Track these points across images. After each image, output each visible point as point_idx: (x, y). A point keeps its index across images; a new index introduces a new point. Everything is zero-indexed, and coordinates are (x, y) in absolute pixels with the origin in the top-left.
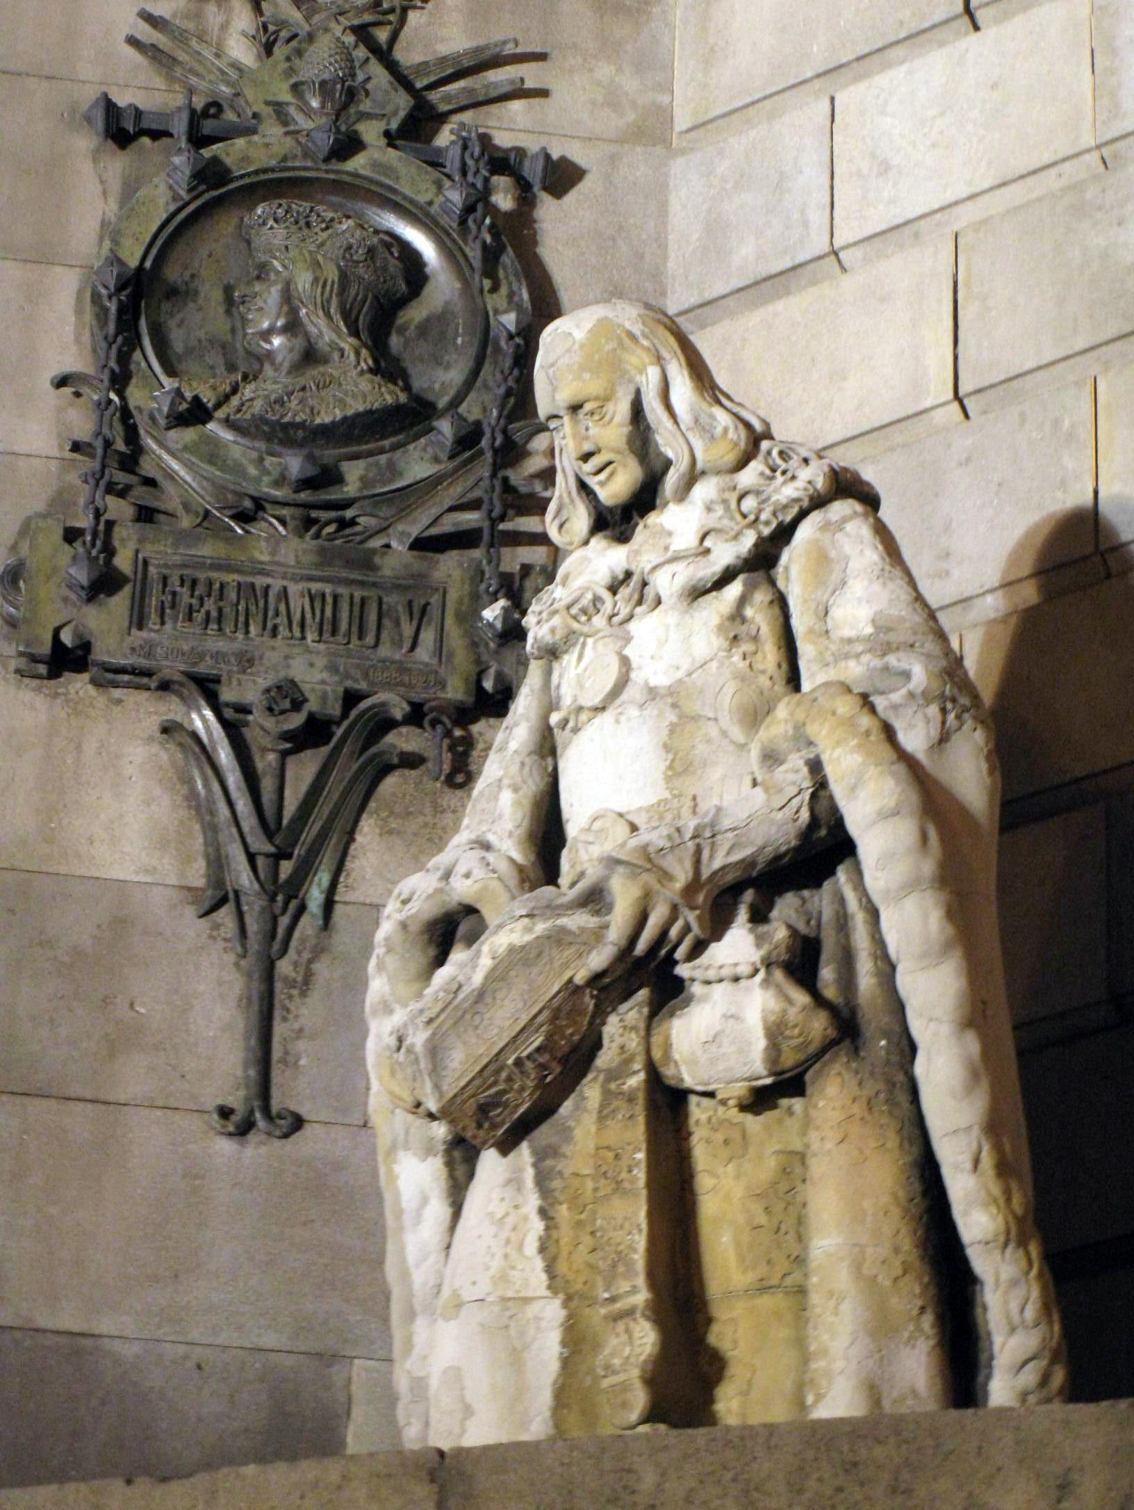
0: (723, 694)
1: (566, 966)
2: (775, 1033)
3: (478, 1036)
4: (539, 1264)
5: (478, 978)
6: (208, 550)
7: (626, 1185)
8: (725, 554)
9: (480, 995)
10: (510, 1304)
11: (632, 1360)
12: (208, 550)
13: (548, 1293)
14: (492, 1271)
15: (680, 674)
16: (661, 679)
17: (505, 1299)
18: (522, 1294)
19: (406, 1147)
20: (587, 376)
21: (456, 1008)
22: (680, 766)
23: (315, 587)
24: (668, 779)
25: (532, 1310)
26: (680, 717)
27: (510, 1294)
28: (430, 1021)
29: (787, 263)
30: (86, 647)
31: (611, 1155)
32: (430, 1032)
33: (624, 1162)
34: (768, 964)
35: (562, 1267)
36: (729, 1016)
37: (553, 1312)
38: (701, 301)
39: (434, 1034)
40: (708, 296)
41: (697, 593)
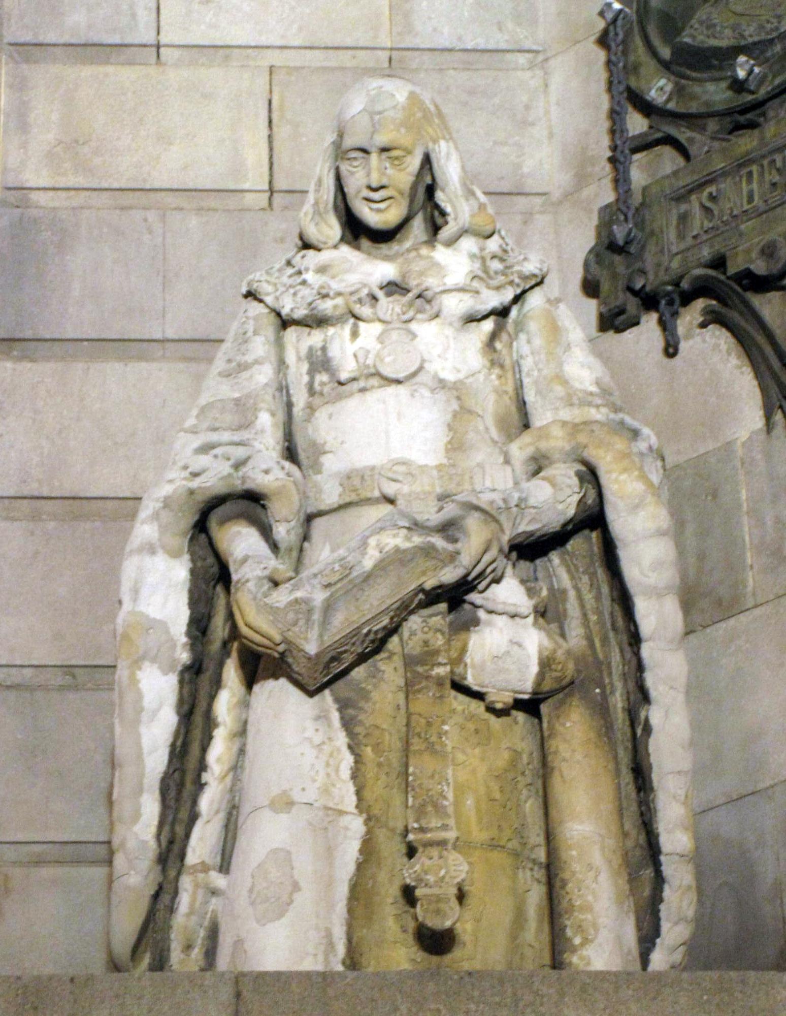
1: (424, 573)
2: (546, 664)
3: (357, 607)
4: (351, 788)
5: (368, 563)
7: (437, 747)
9: (368, 577)
10: (330, 812)
11: (447, 879)
13: (355, 811)
14: (317, 784)
15: (461, 376)
17: (327, 808)
18: (340, 807)
19: (154, 660)
20: (403, 130)
21: (351, 581)
22: (456, 445)
24: (447, 451)
25: (345, 820)
26: (461, 407)
27: (331, 805)
28: (328, 586)
29: (117, 39)
31: (423, 721)
32: (328, 594)
33: (433, 731)
35: (367, 794)
36: (508, 644)
37: (356, 826)
38: (34, 41)
39: (331, 595)
40: (41, 39)
41: (473, 319)
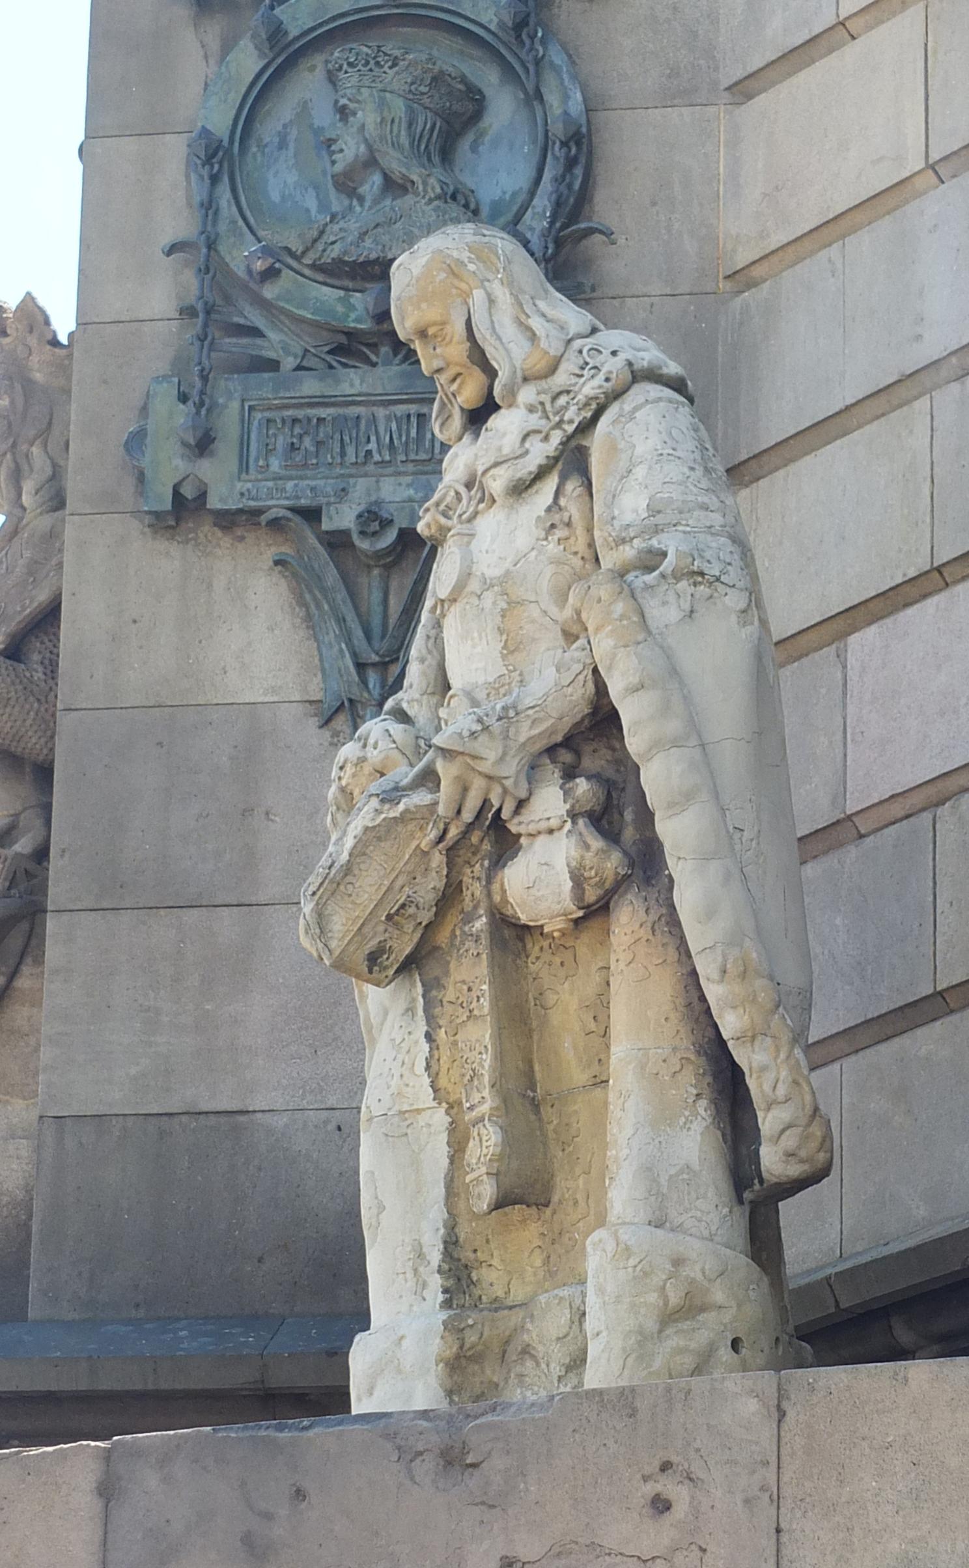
0: (541, 579)
1: (412, 836)
3: (353, 903)
5: (345, 856)
6: (310, 386)
8: (539, 452)
9: (348, 869)
10: (407, 1115)
12: (310, 386)
13: (434, 1104)
15: (508, 564)
16: (493, 572)
18: (415, 1107)
20: (424, 306)
21: (332, 881)
23: (400, 409)
24: (504, 657)
25: (422, 1120)
27: (406, 1108)
28: (314, 893)
29: (805, 36)
30: (202, 496)
31: (465, 987)
33: (474, 994)
34: (573, 815)
37: (440, 1118)
38: (746, 74)
39: (317, 904)
40: (751, 69)
